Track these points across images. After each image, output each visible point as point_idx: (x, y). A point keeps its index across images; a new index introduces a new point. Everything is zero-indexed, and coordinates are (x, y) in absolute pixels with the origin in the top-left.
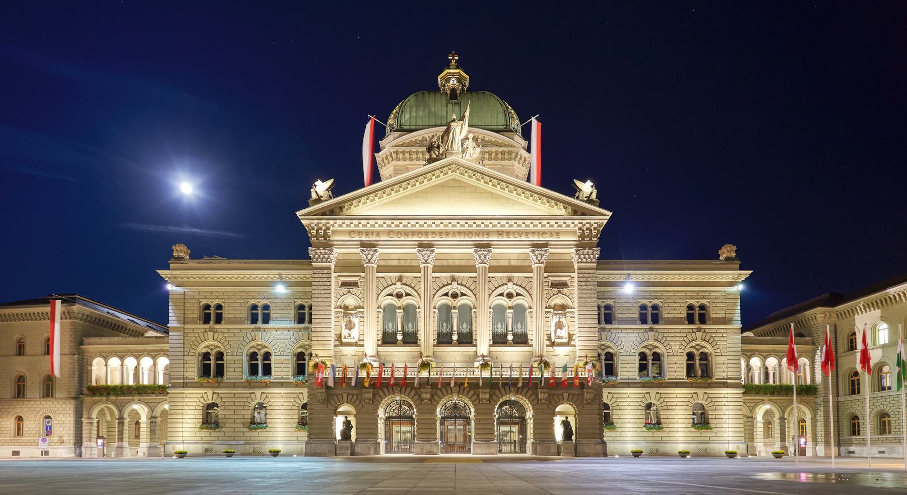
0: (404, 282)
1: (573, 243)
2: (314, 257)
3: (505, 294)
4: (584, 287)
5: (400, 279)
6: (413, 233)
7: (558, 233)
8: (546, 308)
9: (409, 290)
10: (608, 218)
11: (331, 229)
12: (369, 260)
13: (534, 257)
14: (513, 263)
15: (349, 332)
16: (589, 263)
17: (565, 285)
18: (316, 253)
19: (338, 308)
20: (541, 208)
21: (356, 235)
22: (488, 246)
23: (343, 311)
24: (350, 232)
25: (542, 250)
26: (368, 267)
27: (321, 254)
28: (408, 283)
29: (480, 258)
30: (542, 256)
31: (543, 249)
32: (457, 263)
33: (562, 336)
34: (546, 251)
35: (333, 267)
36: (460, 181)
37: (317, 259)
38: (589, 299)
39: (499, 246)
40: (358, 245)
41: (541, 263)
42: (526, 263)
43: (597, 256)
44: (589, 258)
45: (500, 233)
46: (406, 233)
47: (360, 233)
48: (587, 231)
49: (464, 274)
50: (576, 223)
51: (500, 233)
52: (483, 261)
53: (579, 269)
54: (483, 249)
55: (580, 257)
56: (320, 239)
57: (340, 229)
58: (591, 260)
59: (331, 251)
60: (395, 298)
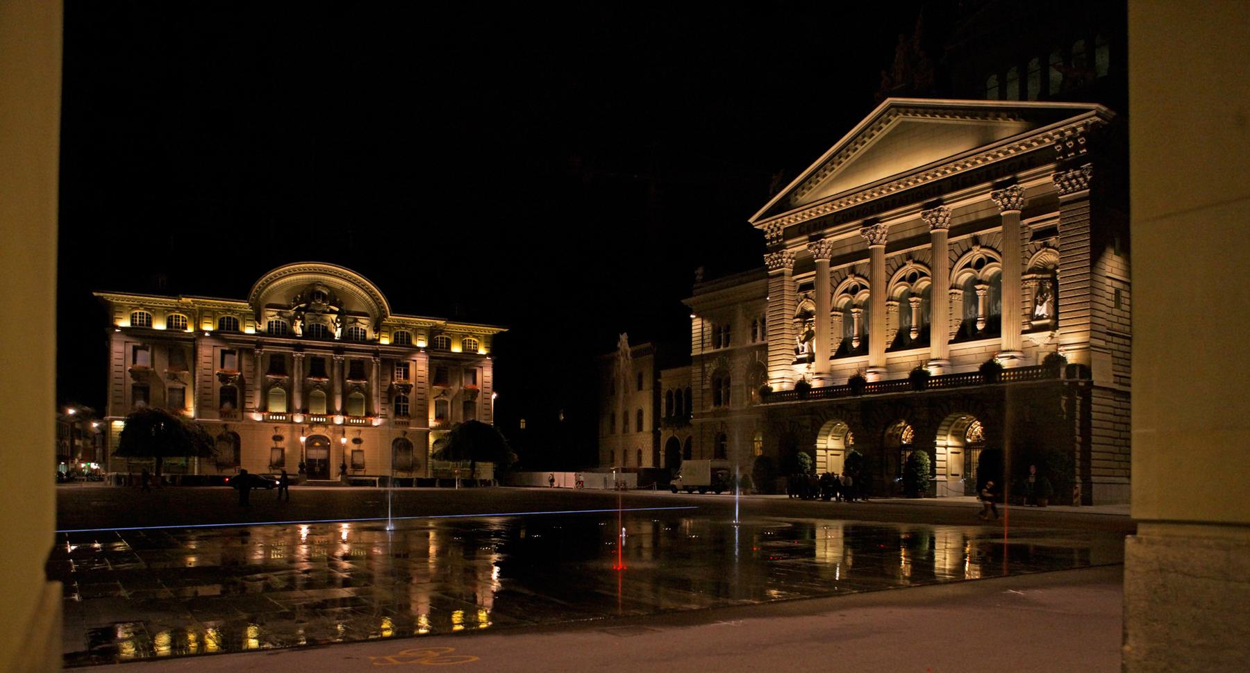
0: (857, 273)
5: (852, 270)
8: (1024, 274)
11: (782, 227)
12: (817, 255)
18: (772, 260)
19: (797, 317)
23: (802, 320)
25: (1007, 190)
26: (818, 263)
27: (776, 259)
28: (862, 273)
30: (1009, 198)
31: (1009, 188)
35: (788, 270)
40: (806, 240)
41: (1009, 209)
43: (1089, 177)
44: (1078, 182)
49: (920, 247)
54: (931, 210)
55: (1063, 186)
56: (773, 242)
58: (1081, 185)
59: (782, 253)
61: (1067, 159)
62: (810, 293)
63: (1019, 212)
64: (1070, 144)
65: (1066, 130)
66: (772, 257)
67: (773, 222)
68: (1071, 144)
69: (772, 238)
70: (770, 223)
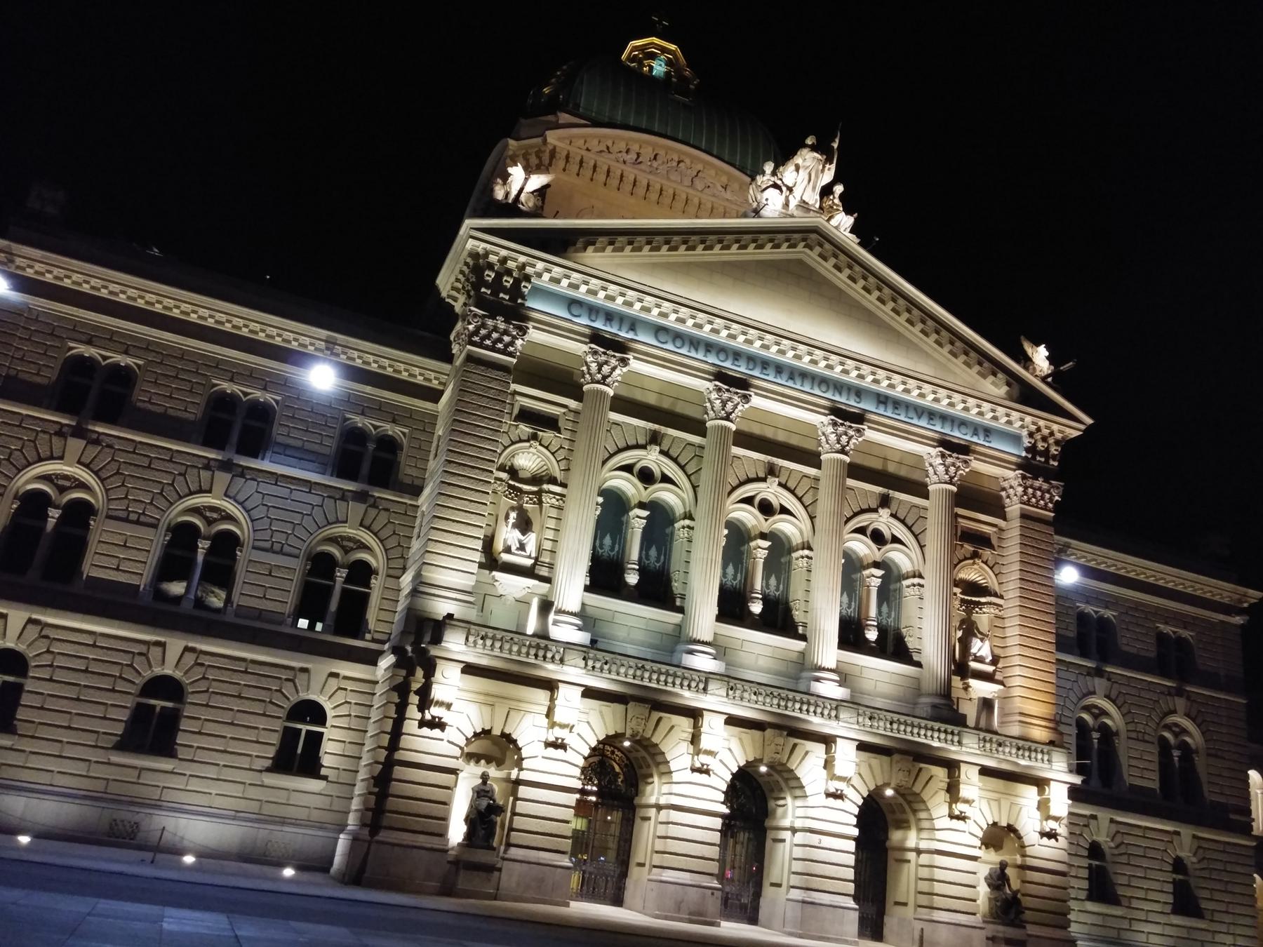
3: (869, 532)
4: (1033, 558)
6: (709, 347)
7: (988, 432)
9: (671, 469)
10: (1083, 427)
12: (605, 378)
13: (941, 469)
14: (892, 468)
18: (484, 326)
21: (584, 312)
24: (572, 303)
27: (495, 329)
29: (838, 441)
30: (958, 468)
31: (961, 456)
32: (781, 437)
33: (981, 657)
36: (812, 270)
37: (483, 338)
38: (1040, 586)
39: (879, 427)
42: (916, 476)
44: (1043, 498)
45: (882, 399)
46: (695, 343)
48: (1043, 444)
50: (1022, 421)
51: (882, 400)
52: (844, 447)
53: (1024, 516)
54: (847, 423)
55: (1025, 493)
56: (501, 295)
58: (1046, 504)
59: (523, 331)
60: (635, 480)
61: (1033, 462)
62: (547, 435)
63: (954, 489)
67: (522, 259)
68: (1043, 446)
69: (497, 285)
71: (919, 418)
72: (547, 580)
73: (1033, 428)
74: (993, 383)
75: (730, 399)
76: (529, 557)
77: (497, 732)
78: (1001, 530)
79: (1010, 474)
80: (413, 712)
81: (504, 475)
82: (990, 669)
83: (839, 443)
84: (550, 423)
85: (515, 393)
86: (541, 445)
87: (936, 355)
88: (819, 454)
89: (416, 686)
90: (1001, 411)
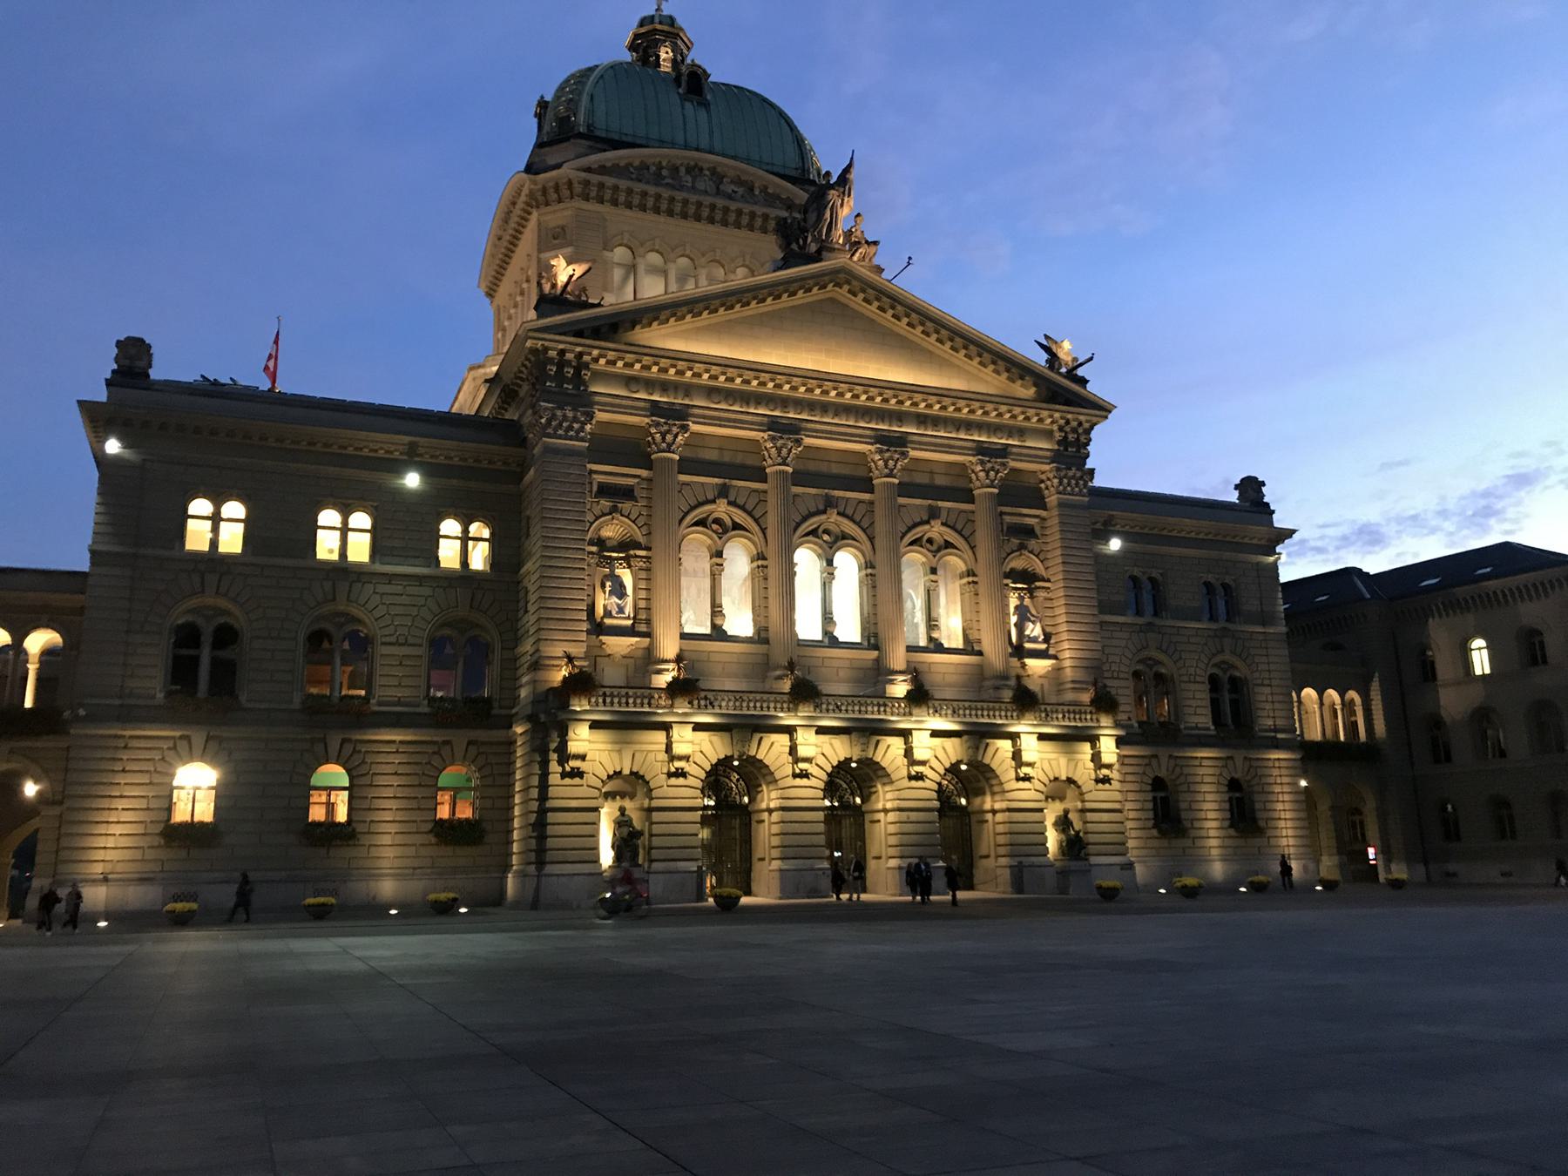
1: (1048, 454)
2: (549, 422)
5: (723, 492)
6: (760, 399)
12: (669, 445)
13: (982, 474)
14: (940, 481)
15: (620, 602)
16: (1076, 495)
17: (1029, 532)
20: (989, 379)
22: (901, 441)
24: (629, 381)
27: (565, 418)
28: (740, 501)
29: (886, 466)
32: (836, 469)
33: (1035, 637)
34: (1004, 464)
44: (1077, 485)
45: (922, 419)
47: (650, 385)
51: (922, 420)
53: (1061, 505)
55: (1061, 483)
56: (565, 386)
57: (611, 369)
58: (1081, 490)
59: (590, 416)
62: (626, 506)
63: (996, 491)
64: (1071, 437)
65: (1074, 420)
66: (559, 413)
67: (579, 349)
70: (587, 350)
71: (958, 430)
72: (648, 635)
73: (1062, 422)
74: (1022, 386)
75: (784, 445)
76: (628, 618)
77: (626, 772)
78: (1044, 519)
79: (1047, 467)
80: (554, 767)
81: (594, 549)
82: (1044, 646)
83: (886, 468)
84: (627, 493)
85: (591, 472)
86: (622, 515)
87: (966, 367)
88: (871, 479)
89: (553, 745)
90: (1031, 412)
